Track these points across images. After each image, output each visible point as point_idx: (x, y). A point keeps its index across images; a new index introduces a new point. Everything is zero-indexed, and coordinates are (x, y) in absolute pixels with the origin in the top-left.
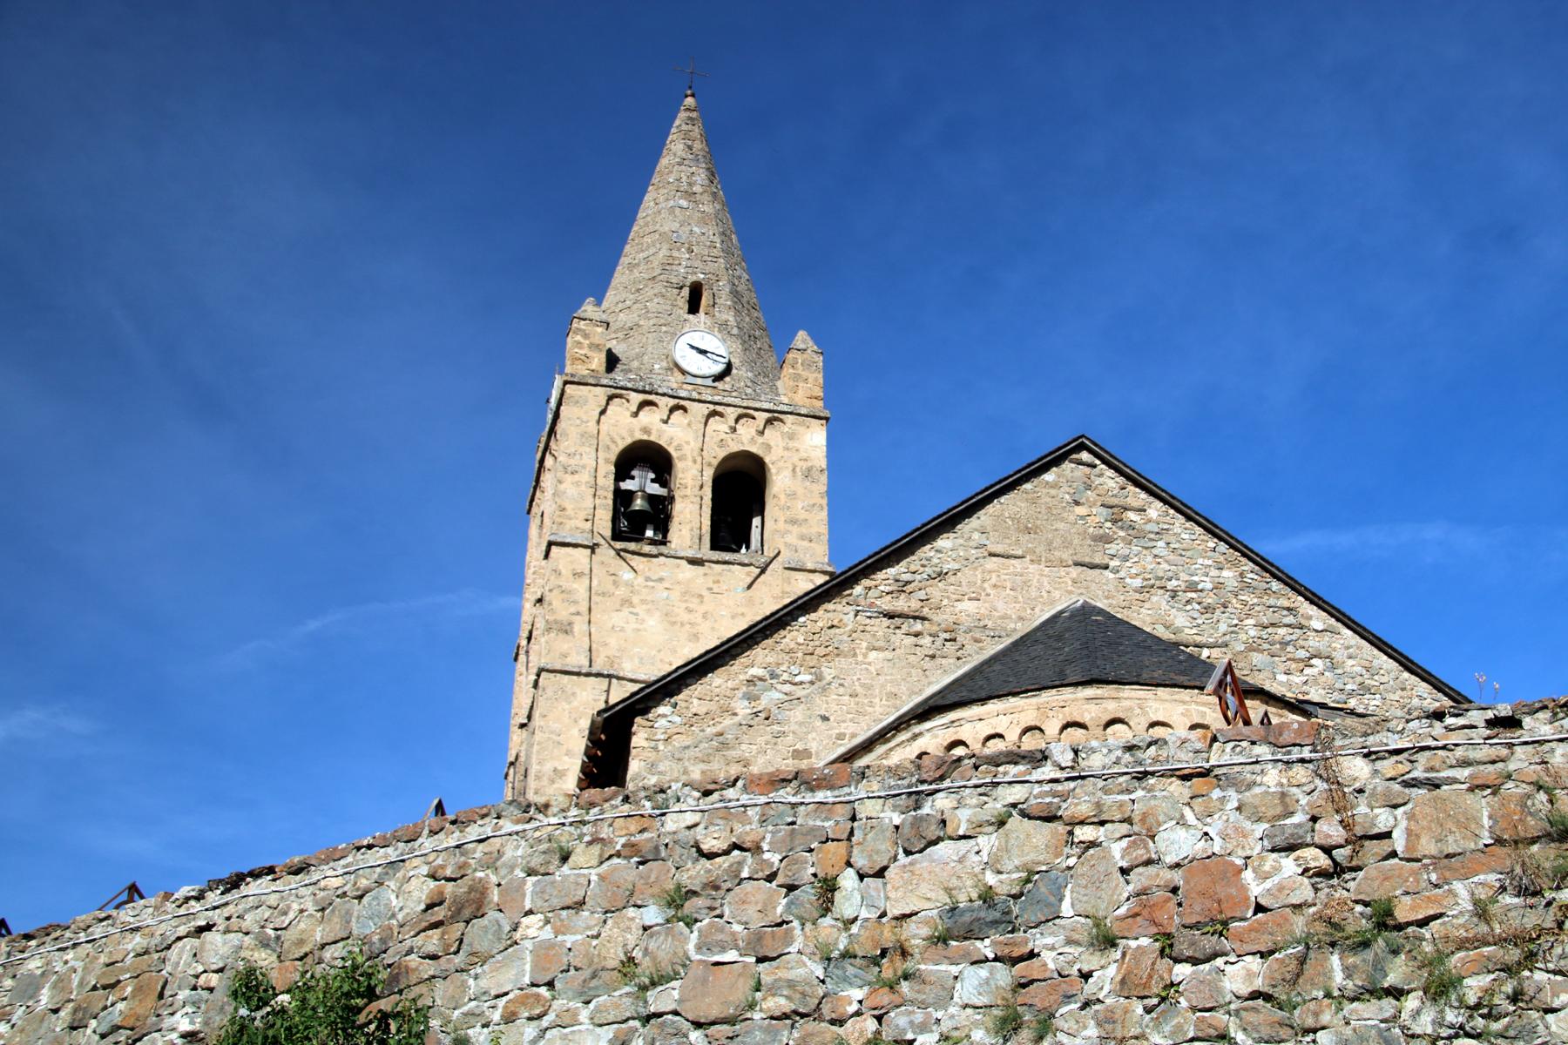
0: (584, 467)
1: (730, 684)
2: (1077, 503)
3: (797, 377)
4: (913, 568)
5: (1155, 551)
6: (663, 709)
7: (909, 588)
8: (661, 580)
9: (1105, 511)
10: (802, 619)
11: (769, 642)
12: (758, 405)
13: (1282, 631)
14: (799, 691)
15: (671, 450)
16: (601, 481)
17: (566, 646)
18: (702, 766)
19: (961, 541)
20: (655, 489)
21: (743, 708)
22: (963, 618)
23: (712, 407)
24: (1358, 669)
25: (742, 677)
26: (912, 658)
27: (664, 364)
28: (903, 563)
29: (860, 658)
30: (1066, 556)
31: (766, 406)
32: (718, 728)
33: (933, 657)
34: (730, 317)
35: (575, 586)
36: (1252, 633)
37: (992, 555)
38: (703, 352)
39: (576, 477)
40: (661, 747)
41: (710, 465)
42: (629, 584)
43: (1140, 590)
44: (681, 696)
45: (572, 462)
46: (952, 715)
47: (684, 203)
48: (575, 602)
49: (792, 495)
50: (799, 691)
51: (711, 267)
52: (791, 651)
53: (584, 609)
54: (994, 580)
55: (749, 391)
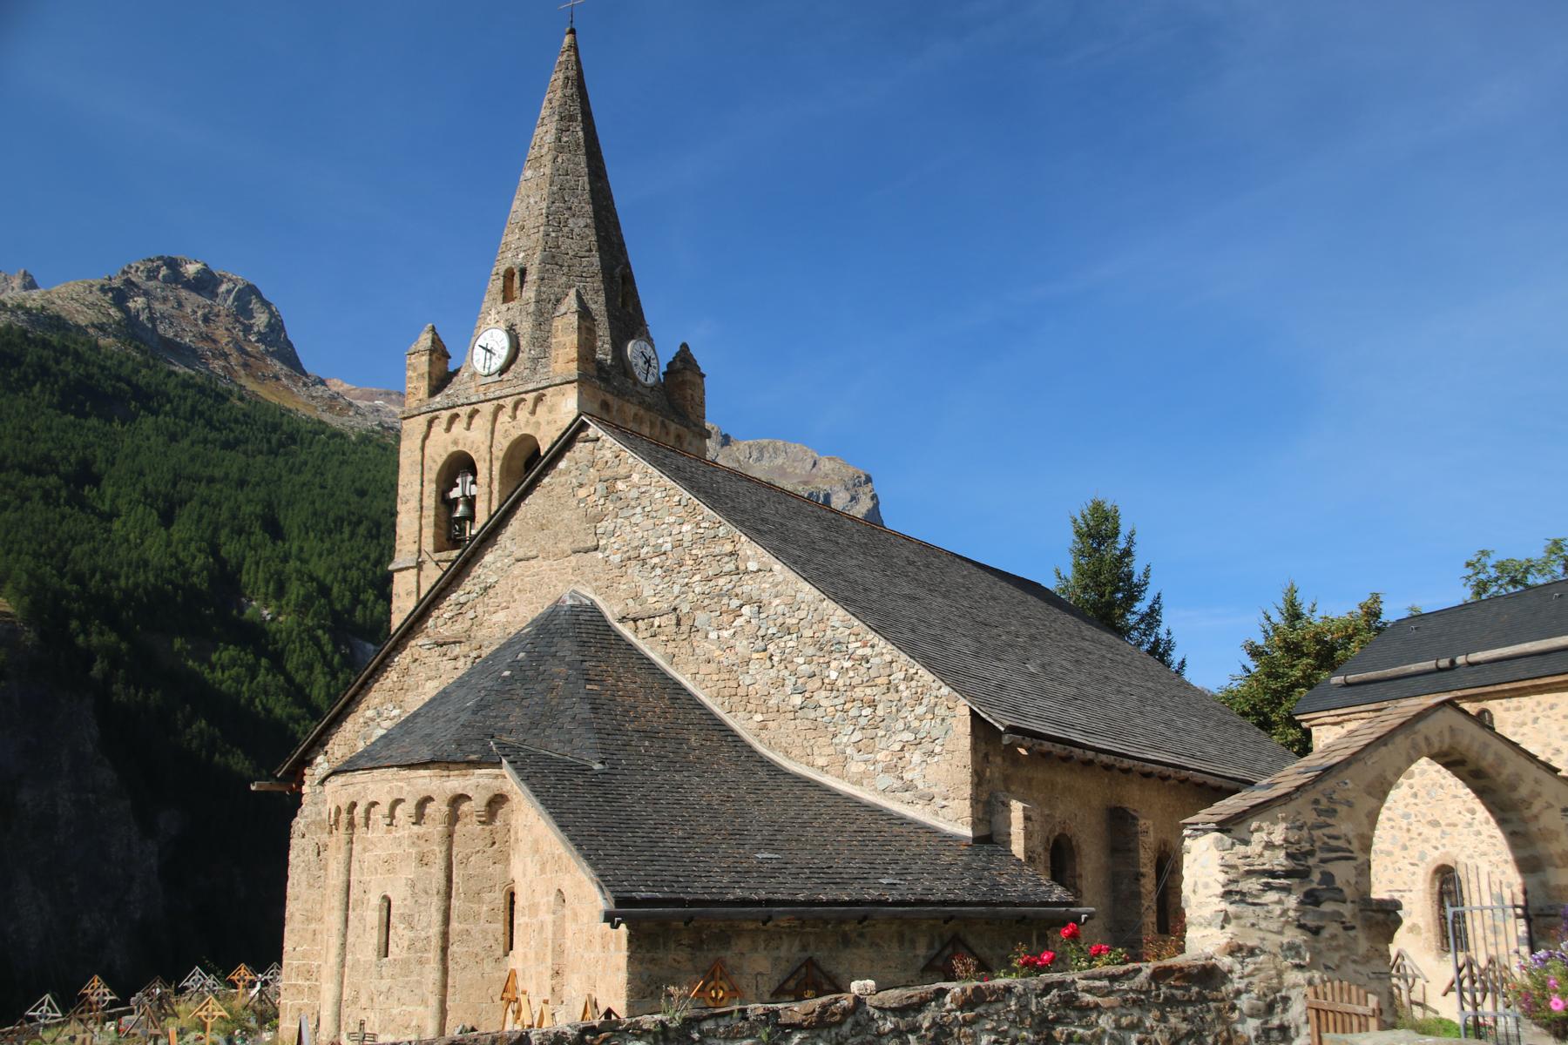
2: (581, 485)
5: (633, 520)
6: (320, 759)
9: (599, 486)
13: (722, 581)
24: (780, 609)
30: (566, 546)
31: (531, 386)
36: (697, 590)
43: (622, 565)
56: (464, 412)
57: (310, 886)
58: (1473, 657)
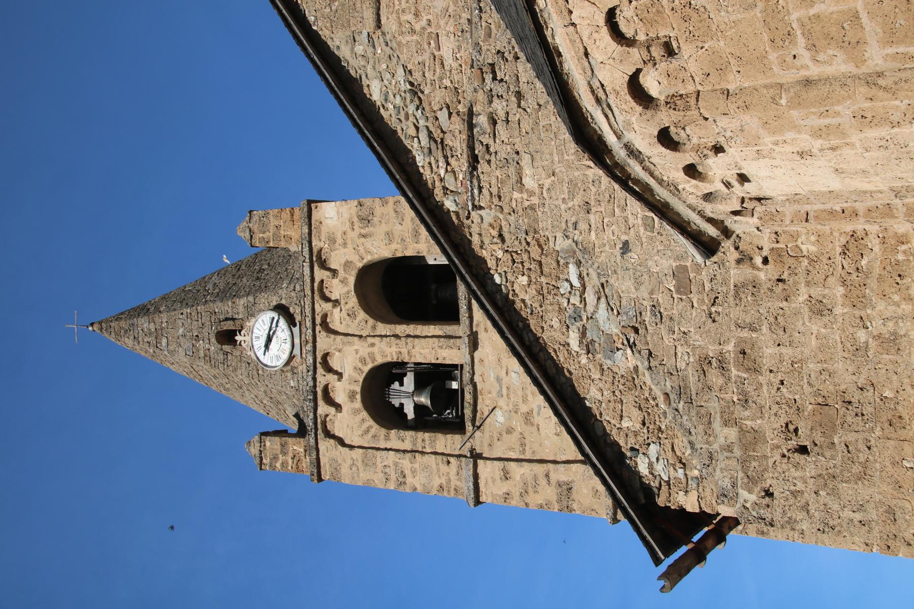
0: (396, 464)
1: (596, 375)
3: (276, 236)
4: (412, 131)
6: (643, 468)
7: (437, 134)
8: (499, 380)
10: (498, 280)
11: (533, 323)
12: (307, 279)
14: (593, 281)
15: (366, 369)
16: (407, 446)
17: (585, 491)
18: (717, 424)
19: (369, 69)
20: (409, 381)
21: (626, 361)
22: (463, 54)
23: (318, 328)
25: (584, 360)
26: (525, 126)
27: (289, 375)
28: (407, 142)
29: (535, 200)
31: (307, 271)
32: (661, 399)
33: (519, 95)
34: (242, 302)
35: (518, 478)
37: (379, 25)
38: (269, 340)
39: (408, 472)
40: (696, 473)
41: (374, 327)
44: (622, 443)
45: (393, 476)
46: (587, 102)
47: (164, 341)
48: (535, 478)
49: (389, 236)
50: (593, 281)
51: (206, 319)
52: (540, 292)
53: (539, 469)
54: (410, 17)
55: (298, 288)
56: (323, 378)
57: (863, 477)
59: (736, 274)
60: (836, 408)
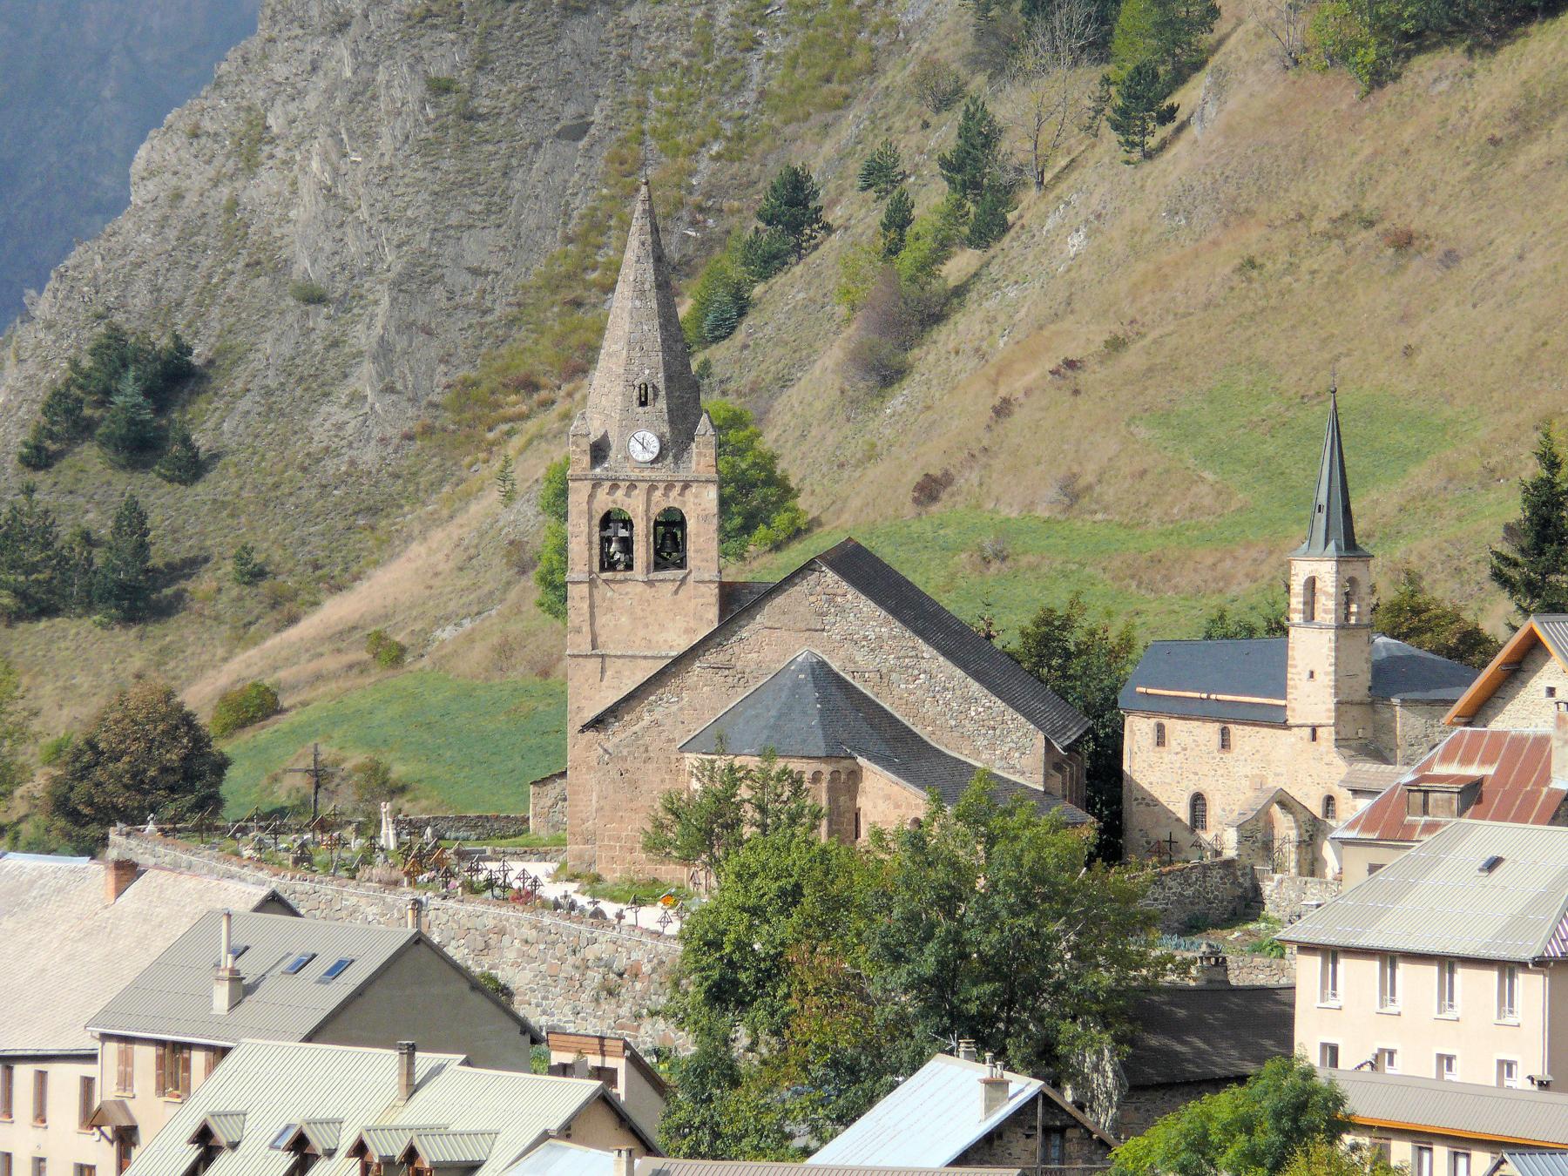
42: (611, 600)
58: (1220, 697)
59: (673, 757)
60: (634, 785)
